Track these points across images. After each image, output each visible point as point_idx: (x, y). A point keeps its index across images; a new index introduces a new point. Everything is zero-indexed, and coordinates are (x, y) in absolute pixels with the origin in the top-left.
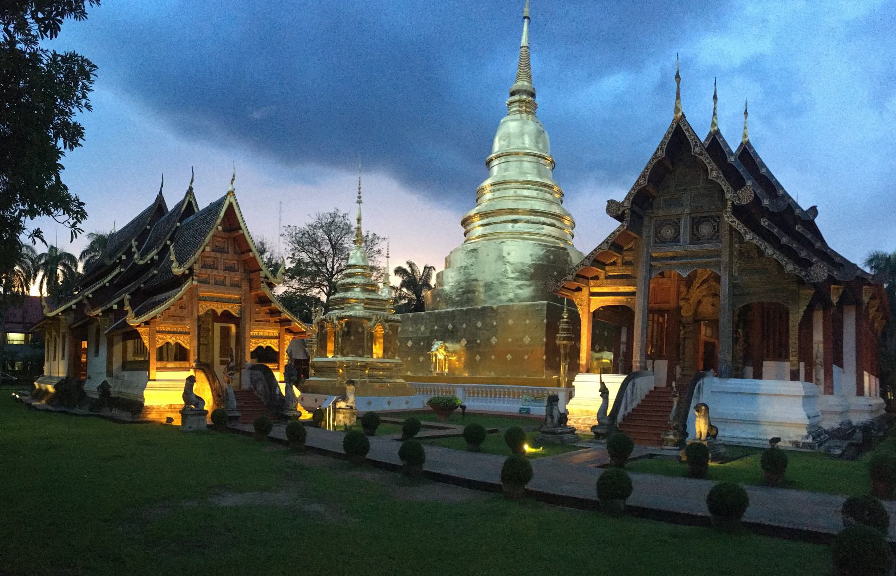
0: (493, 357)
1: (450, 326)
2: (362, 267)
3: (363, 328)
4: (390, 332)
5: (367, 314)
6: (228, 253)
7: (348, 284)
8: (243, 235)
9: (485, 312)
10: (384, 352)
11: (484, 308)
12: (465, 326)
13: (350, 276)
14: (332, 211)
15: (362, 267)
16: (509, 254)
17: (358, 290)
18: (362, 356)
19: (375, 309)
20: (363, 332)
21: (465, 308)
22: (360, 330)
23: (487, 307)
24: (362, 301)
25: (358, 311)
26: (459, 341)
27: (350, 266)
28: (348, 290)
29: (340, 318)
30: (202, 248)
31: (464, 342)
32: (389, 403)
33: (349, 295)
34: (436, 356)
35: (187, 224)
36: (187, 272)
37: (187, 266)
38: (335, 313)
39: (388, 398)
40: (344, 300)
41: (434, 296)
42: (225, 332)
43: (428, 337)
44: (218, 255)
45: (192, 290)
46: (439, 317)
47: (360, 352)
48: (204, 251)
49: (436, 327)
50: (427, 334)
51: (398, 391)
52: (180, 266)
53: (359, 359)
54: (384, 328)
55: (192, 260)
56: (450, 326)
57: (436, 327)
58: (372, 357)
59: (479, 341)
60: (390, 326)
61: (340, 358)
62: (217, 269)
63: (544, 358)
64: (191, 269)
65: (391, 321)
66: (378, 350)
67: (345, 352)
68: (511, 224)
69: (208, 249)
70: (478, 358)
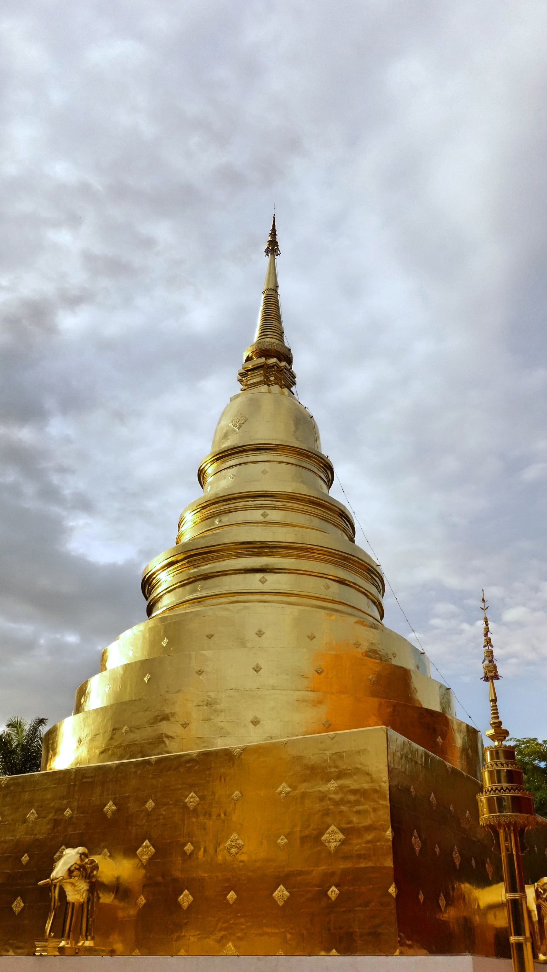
0: (232, 896)
1: (110, 807)
9: (211, 765)
11: (207, 757)
12: (150, 804)
16: (260, 634)
21: (153, 758)
23: (216, 754)
26: (130, 851)
31: (146, 850)
49: (68, 812)
56: (110, 807)
57: (68, 812)
59: (189, 848)
63: (392, 890)
68: (259, 576)
70: (185, 898)
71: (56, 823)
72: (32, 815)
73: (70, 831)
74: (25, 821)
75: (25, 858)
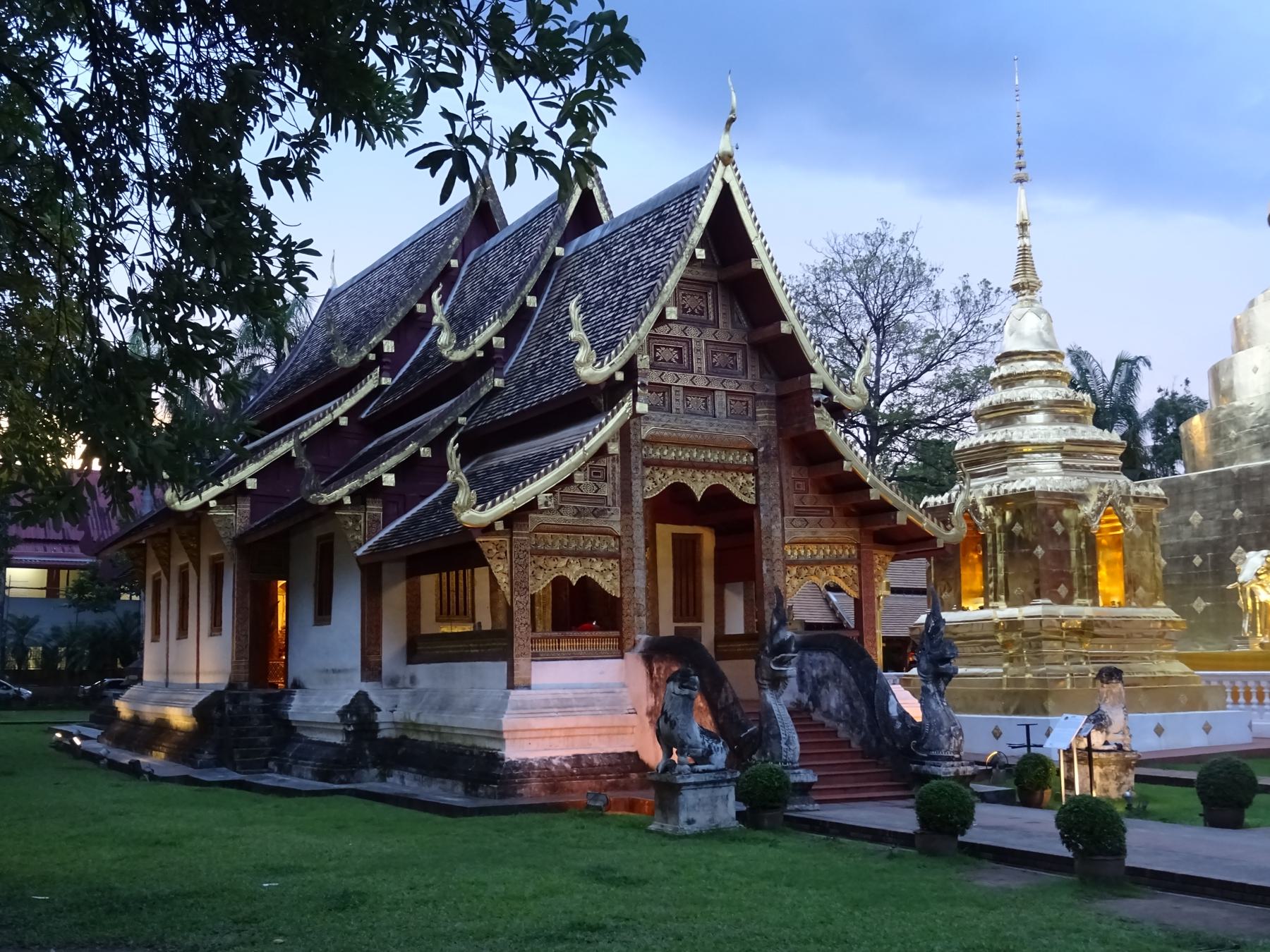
2: (1044, 356)
3: (1064, 522)
4: (1139, 532)
5: (1072, 483)
6: (715, 324)
7: (1012, 404)
8: (761, 273)
10: (1126, 590)
13: (1009, 381)
14: (871, 230)
15: (1044, 356)
17: (1040, 417)
18: (1067, 601)
19: (1086, 470)
20: (1065, 536)
22: (1058, 528)
24: (1058, 448)
25: (1044, 476)
27: (1007, 357)
28: (1008, 421)
29: (991, 500)
30: (656, 311)
32: (1159, 731)
33: (1016, 433)
34: (1253, 595)
35: (582, 252)
36: (620, 376)
37: (619, 359)
38: (983, 487)
39: (1155, 717)
40: (1005, 450)
41: (1217, 432)
42: (686, 552)
43: (1215, 546)
44: (692, 332)
45: (624, 432)
46: (1243, 484)
47: (1063, 590)
48: (662, 319)
49: (1238, 514)
50: (1213, 536)
51: (1164, 695)
52: (600, 358)
53: (1062, 610)
54: (1123, 519)
55: (631, 343)
57: (1238, 514)
58: (1096, 604)
60: (1137, 513)
61: (1004, 611)
62: (690, 370)
64: (630, 368)
65: (1137, 499)
66: (1110, 584)
67: (1016, 591)
69: (672, 313)
71: (1226, 525)
72: (1196, 517)
73: (1244, 532)
74: (1189, 524)
75: (1197, 561)
